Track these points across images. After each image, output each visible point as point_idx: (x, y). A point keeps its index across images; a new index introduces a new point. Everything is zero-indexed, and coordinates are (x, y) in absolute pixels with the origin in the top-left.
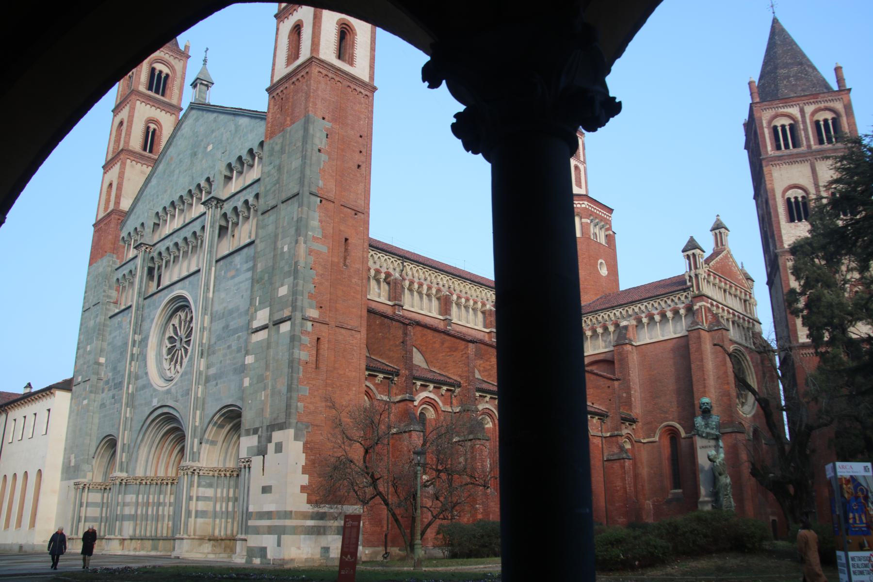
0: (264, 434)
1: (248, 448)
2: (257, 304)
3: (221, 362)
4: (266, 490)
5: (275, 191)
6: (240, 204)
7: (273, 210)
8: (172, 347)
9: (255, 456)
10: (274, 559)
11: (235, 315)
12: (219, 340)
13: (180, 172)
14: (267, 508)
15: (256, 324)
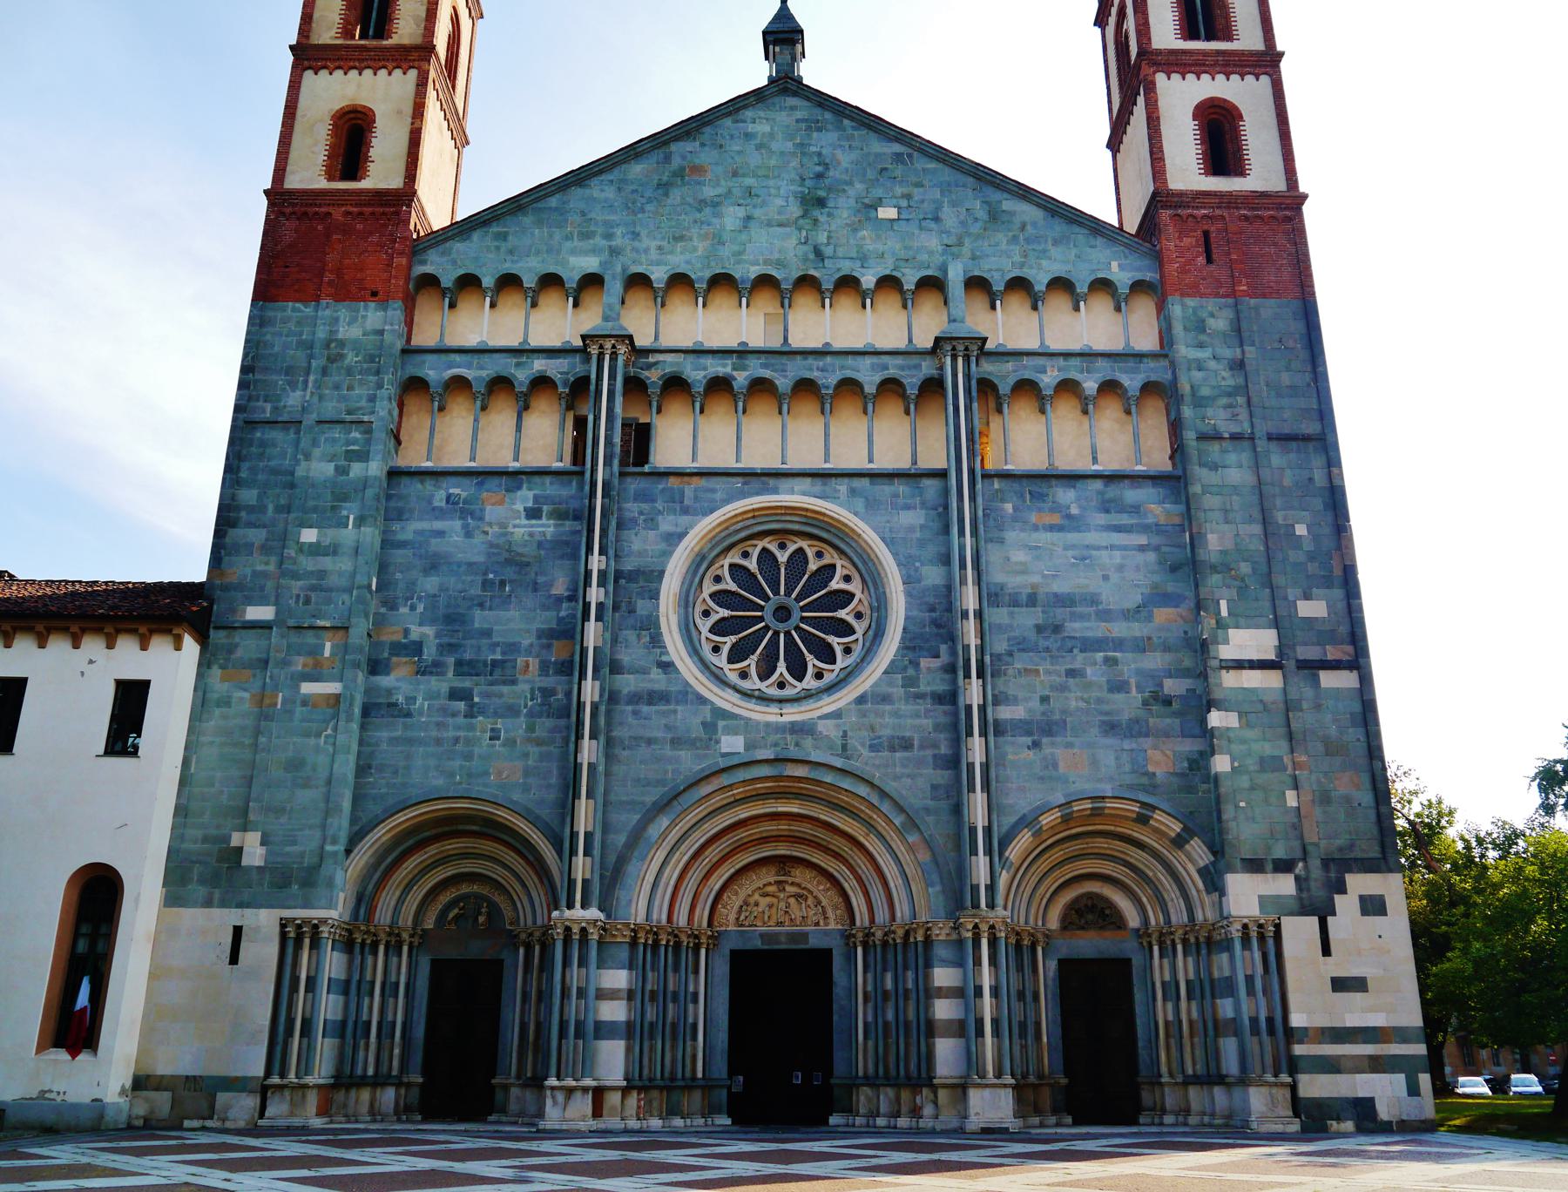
0: (1316, 872)
1: (1260, 897)
2: (1224, 612)
3: (1045, 699)
4: (1339, 984)
5: (1230, 406)
6: (1049, 378)
7: (1236, 442)
8: (732, 617)
9: (1292, 914)
10: (1403, 1121)
11: (1079, 609)
12: (1023, 650)
13: (749, 218)
14: (1352, 1020)
15: (1226, 652)
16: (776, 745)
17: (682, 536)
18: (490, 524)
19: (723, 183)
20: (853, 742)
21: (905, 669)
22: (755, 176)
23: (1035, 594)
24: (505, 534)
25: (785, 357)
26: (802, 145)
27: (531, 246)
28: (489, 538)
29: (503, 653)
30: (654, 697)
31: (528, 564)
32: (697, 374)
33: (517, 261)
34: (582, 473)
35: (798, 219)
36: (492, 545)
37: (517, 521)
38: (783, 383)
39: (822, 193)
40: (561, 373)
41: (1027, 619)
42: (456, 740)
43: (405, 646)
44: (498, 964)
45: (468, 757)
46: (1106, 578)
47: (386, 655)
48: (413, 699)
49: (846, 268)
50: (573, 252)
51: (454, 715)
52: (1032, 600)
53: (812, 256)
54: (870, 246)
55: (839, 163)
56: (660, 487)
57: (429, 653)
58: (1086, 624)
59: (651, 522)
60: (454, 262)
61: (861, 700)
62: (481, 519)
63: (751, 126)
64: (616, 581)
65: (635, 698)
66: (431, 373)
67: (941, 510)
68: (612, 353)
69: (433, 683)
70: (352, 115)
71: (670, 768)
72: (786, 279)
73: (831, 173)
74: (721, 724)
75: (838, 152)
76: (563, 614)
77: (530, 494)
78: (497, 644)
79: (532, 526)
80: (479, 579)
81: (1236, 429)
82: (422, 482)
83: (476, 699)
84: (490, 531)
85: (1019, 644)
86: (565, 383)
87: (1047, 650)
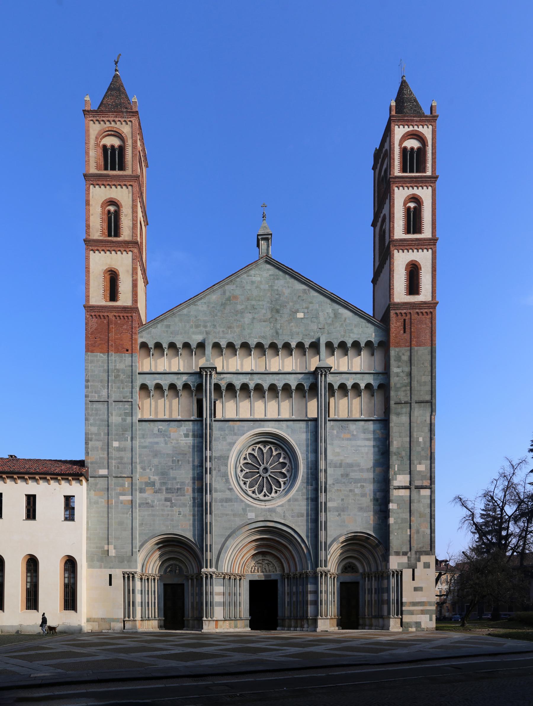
12: (337, 483)
13: (254, 318)
16: (264, 516)
17: (234, 443)
18: (173, 440)
19: (244, 303)
20: (287, 515)
21: (303, 489)
22: (256, 300)
23: (341, 463)
24: (178, 443)
25: (266, 375)
26: (271, 286)
27: (179, 331)
28: (173, 444)
29: (180, 485)
30: (228, 500)
31: (186, 454)
32: (238, 382)
33: (174, 337)
34: (202, 421)
35: (270, 318)
36: (174, 447)
37: (181, 439)
38: (266, 386)
39: (278, 307)
40: (192, 382)
41: (340, 471)
42: (168, 515)
43: (150, 483)
44: (183, 585)
45: (172, 520)
46: (363, 457)
47: (144, 486)
48: (153, 501)
49: (287, 339)
50: (194, 333)
51: (167, 507)
52: (341, 466)
53: (275, 334)
54: (295, 330)
55: (284, 294)
56: (227, 425)
57: (157, 486)
58: (356, 474)
59: (224, 439)
60: (153, 338)
61: (289, 501)
62: (170, 437)
63: (254, 278)
64: (214, 460)
65: (222, 501)
66: (149, 382)
67: (314, 433)
68: (210, 374)
69: (159, 496)
70: (113, 273)
71: (233, 523)
72: (266, 344)
73: (281, 299)
74: (248, 509)
75: (284, 289)
76: (198, 472)
77: (185, 428)
78: (178, 482)
79: (186, 440)
80: (171, 459)
81: (406, 400)
82: (149, 424)
83: (173, 501)
84: (173, 442)
85: (336, 481)
86: (194, 385)
87: (344, 483)
